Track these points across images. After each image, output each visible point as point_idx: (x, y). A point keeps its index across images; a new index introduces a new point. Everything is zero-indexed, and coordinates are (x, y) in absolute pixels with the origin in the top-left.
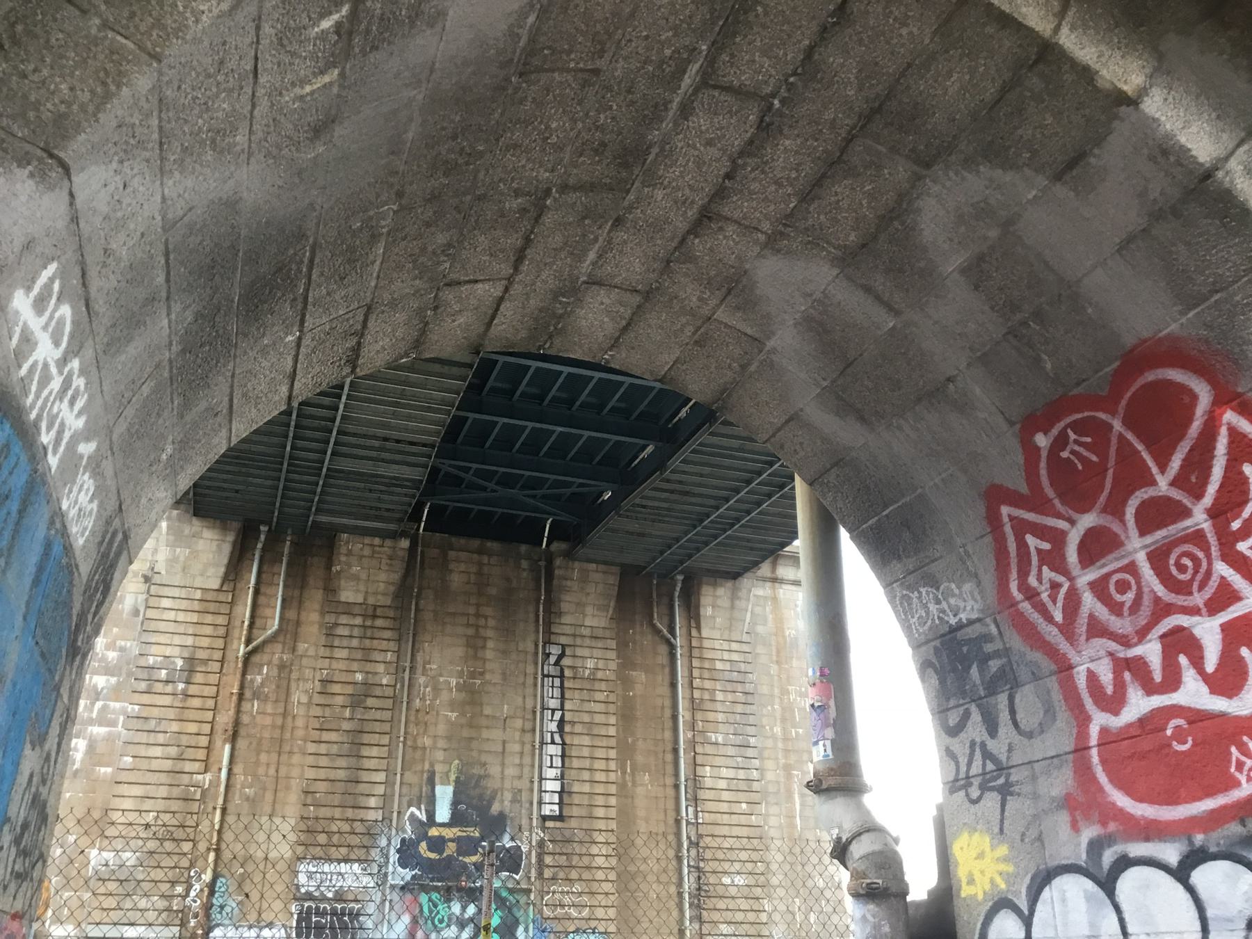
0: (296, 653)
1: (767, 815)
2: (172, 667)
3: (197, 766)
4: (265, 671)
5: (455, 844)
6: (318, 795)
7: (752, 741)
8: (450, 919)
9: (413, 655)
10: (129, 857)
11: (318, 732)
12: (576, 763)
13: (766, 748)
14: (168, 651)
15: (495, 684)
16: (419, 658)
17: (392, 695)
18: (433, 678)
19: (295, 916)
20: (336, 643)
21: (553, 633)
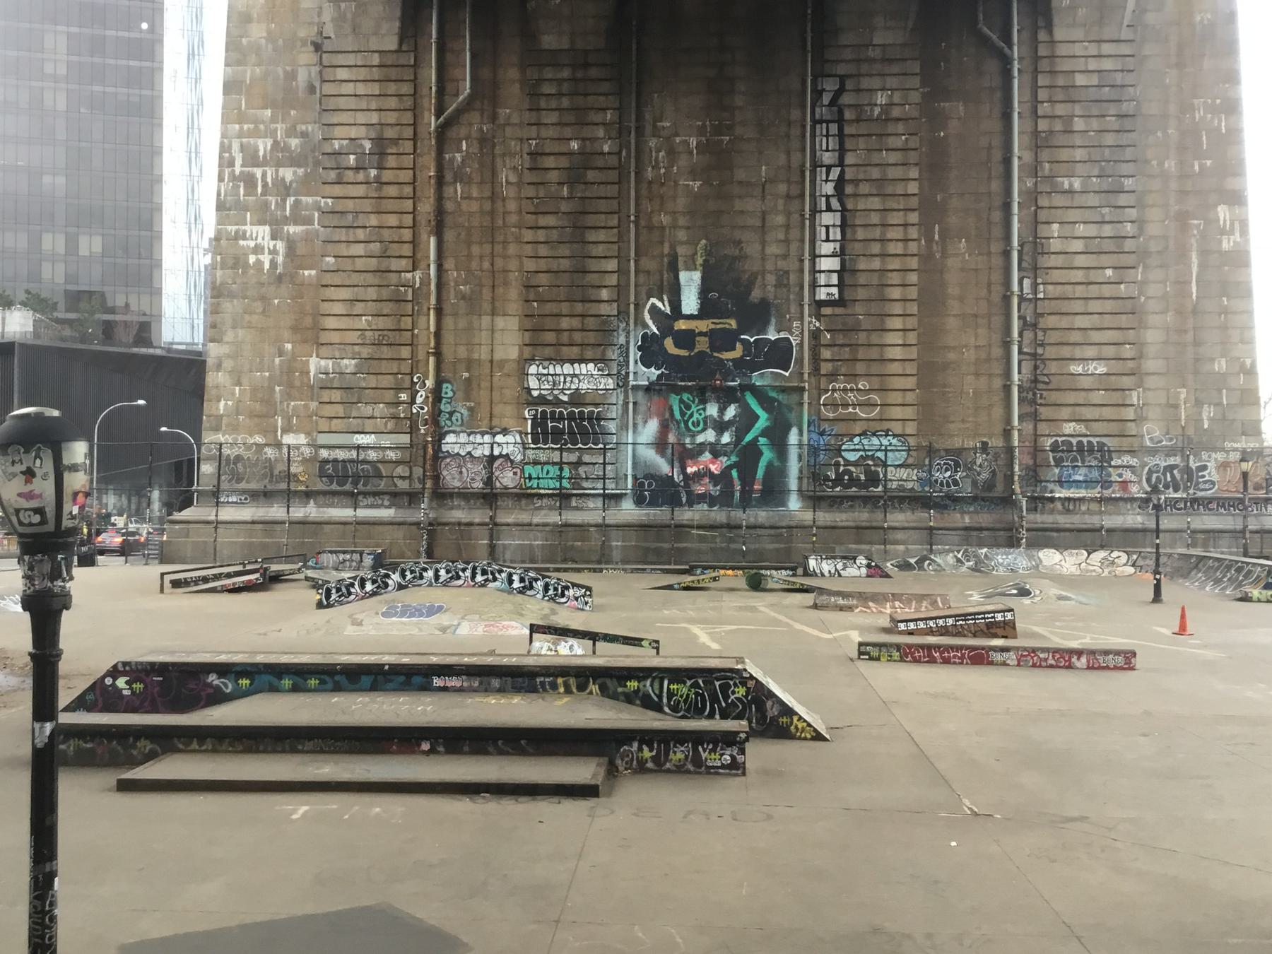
0: (497, 122)
1: (1144, 282)
2: (359, 151)
3: (404, 263)
4: (464, 148)
5: (707, 339)
6: (541, 289)
7: (1128, 183)
8: (705, 423)
9: (638, 107)
10: (349, 364)
11: (534, 216)
12: (861, 234)
13: (1151, 192)
14: (354, 132)
15: (749, 140)
16: (647, 116)
17: (617, 165)
18: (668, 139)
19: (530, 422)
20: (543, 104)
21: (828, 61)
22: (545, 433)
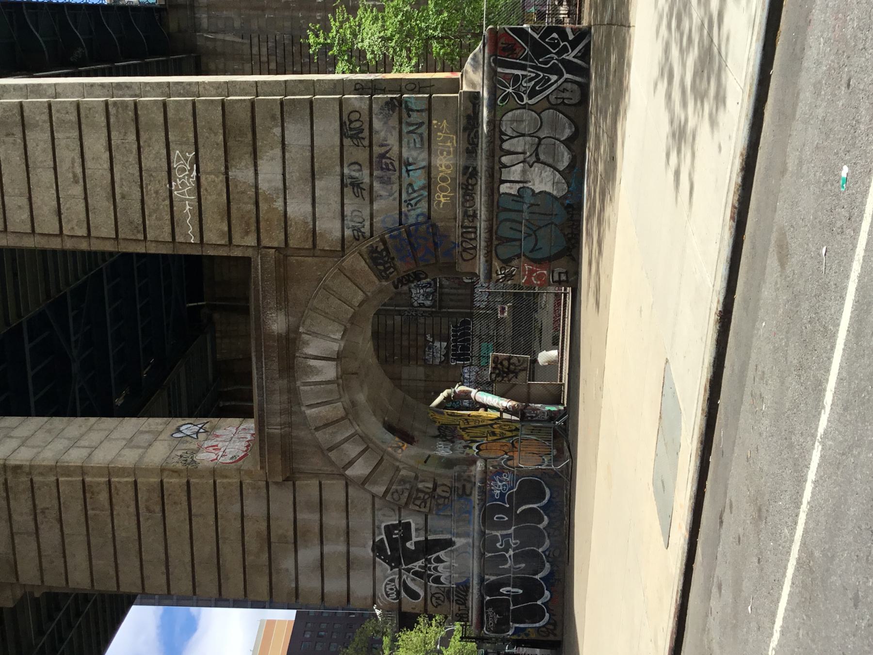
19: (458, 362)
22: (463, 355)
